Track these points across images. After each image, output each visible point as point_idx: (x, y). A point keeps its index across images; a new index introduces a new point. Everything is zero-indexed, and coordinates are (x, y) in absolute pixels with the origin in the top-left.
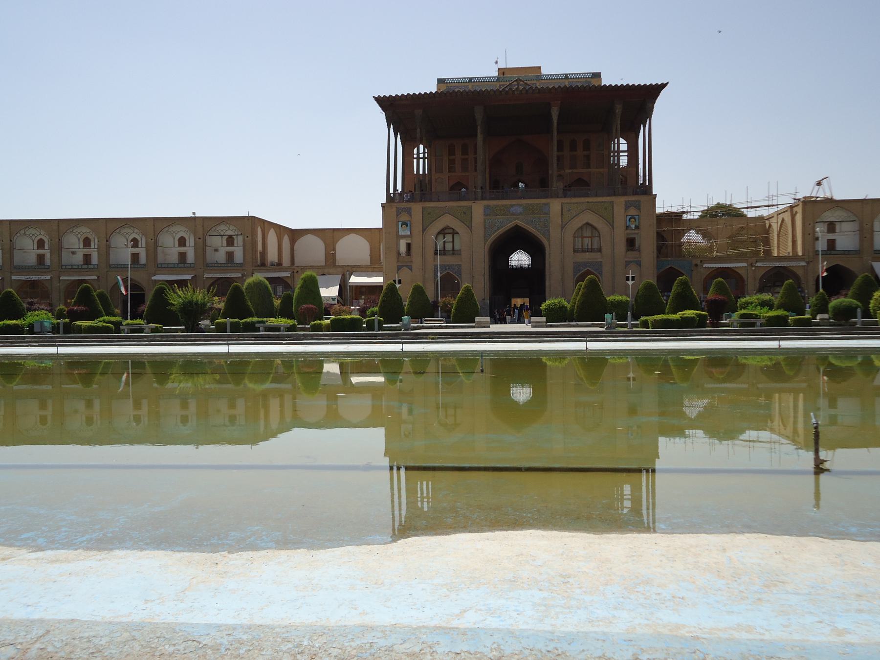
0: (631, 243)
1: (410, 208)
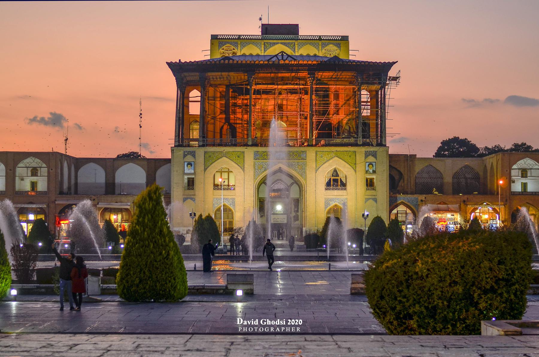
0: (370, 184)
1: (195, 152)
